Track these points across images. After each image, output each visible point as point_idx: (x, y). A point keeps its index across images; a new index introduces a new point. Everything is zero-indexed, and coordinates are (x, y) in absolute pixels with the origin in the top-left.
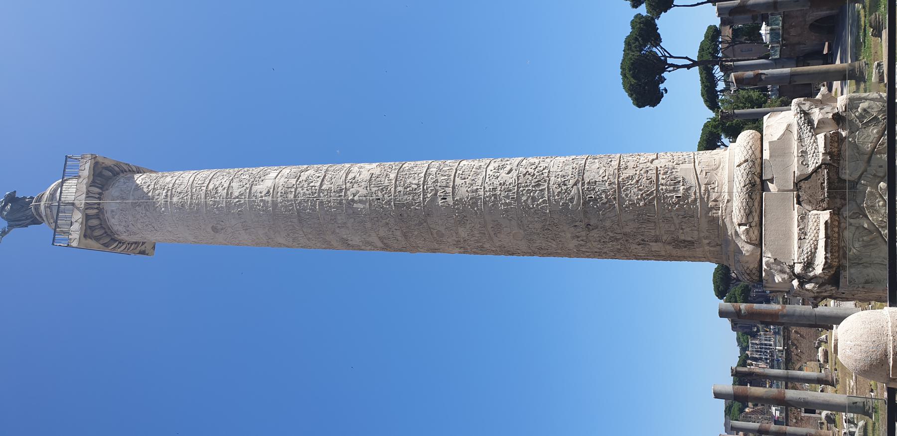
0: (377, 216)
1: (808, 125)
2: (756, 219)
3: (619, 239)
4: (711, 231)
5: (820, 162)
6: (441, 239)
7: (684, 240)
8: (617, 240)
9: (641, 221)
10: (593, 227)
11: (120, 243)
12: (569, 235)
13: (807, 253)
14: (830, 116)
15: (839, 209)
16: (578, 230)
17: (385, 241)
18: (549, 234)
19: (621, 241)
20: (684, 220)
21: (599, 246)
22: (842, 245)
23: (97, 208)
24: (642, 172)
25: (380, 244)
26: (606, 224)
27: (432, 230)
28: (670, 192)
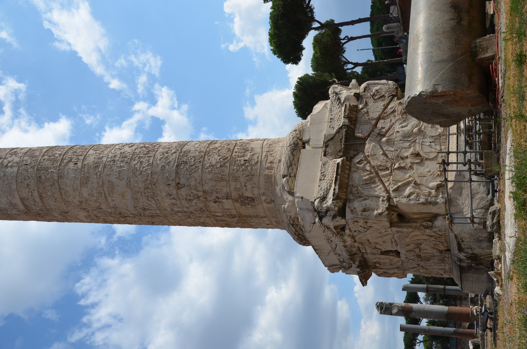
1: (337, 101)
5: (341, 124)
7: (247, 197)
9: (217, 179)
12: (164, 194)
13: (324, 190)
14: (353, 94)
15: (352, 158)
17: (26, 203)
18: (149, 193)
19: (201, 198)
21: (186, 205)
22: (351, 183)
24: (225, 145)
25: (21, 207)
27: (62, 191)
28: (241, 157)
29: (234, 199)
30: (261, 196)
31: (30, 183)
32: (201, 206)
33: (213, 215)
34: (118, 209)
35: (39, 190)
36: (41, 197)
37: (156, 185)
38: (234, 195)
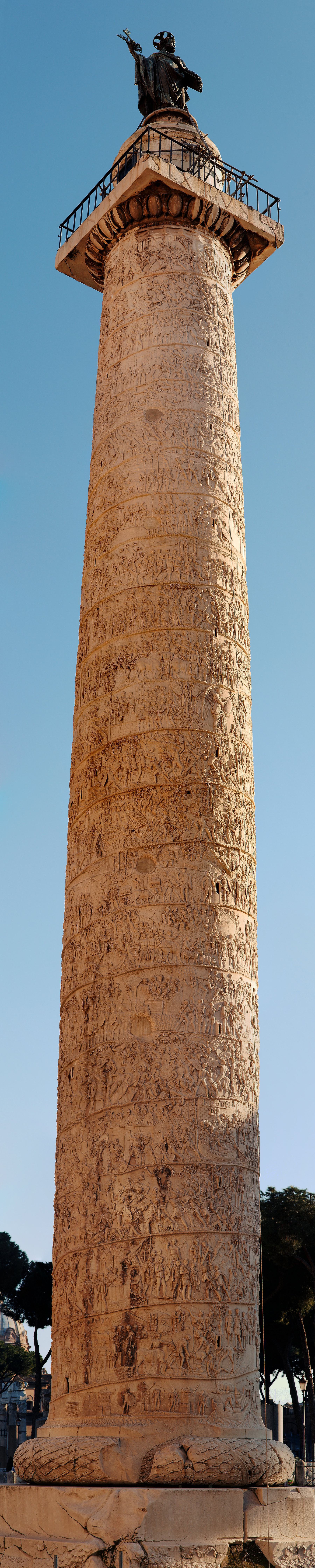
0: (186, 743)
2: (198, 1478)
3: (138, 1228)
4: (156, 1397)
6: (134, 865)
8: (136, 1223)
10: (164, 1180)
11: (119, 230)
12: (145, 1132)
16: (158, 1151)
17: (126, 748)
19: (132, 1229)
20: (180, 1350)
23: (198, 219)
25: (117, 732)
26: (169, 1207)
27: (156, 851)
29: (132, 1316)
30: (139, 1382)
31: (174, 765)
32: (114, 1226)
33: (90, 1252)
34: (107, 996)
35: (158, 789)
36: (141, 791)
37: (166, 1112)
38: (142, 1316)
